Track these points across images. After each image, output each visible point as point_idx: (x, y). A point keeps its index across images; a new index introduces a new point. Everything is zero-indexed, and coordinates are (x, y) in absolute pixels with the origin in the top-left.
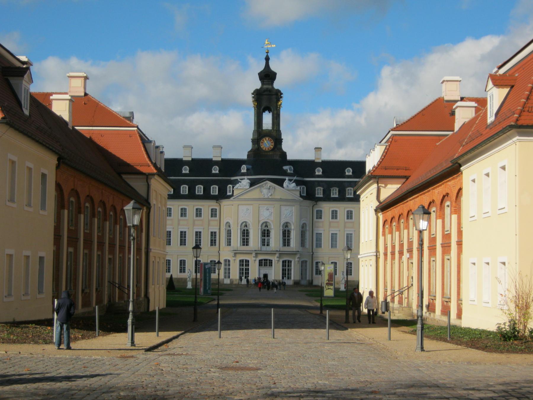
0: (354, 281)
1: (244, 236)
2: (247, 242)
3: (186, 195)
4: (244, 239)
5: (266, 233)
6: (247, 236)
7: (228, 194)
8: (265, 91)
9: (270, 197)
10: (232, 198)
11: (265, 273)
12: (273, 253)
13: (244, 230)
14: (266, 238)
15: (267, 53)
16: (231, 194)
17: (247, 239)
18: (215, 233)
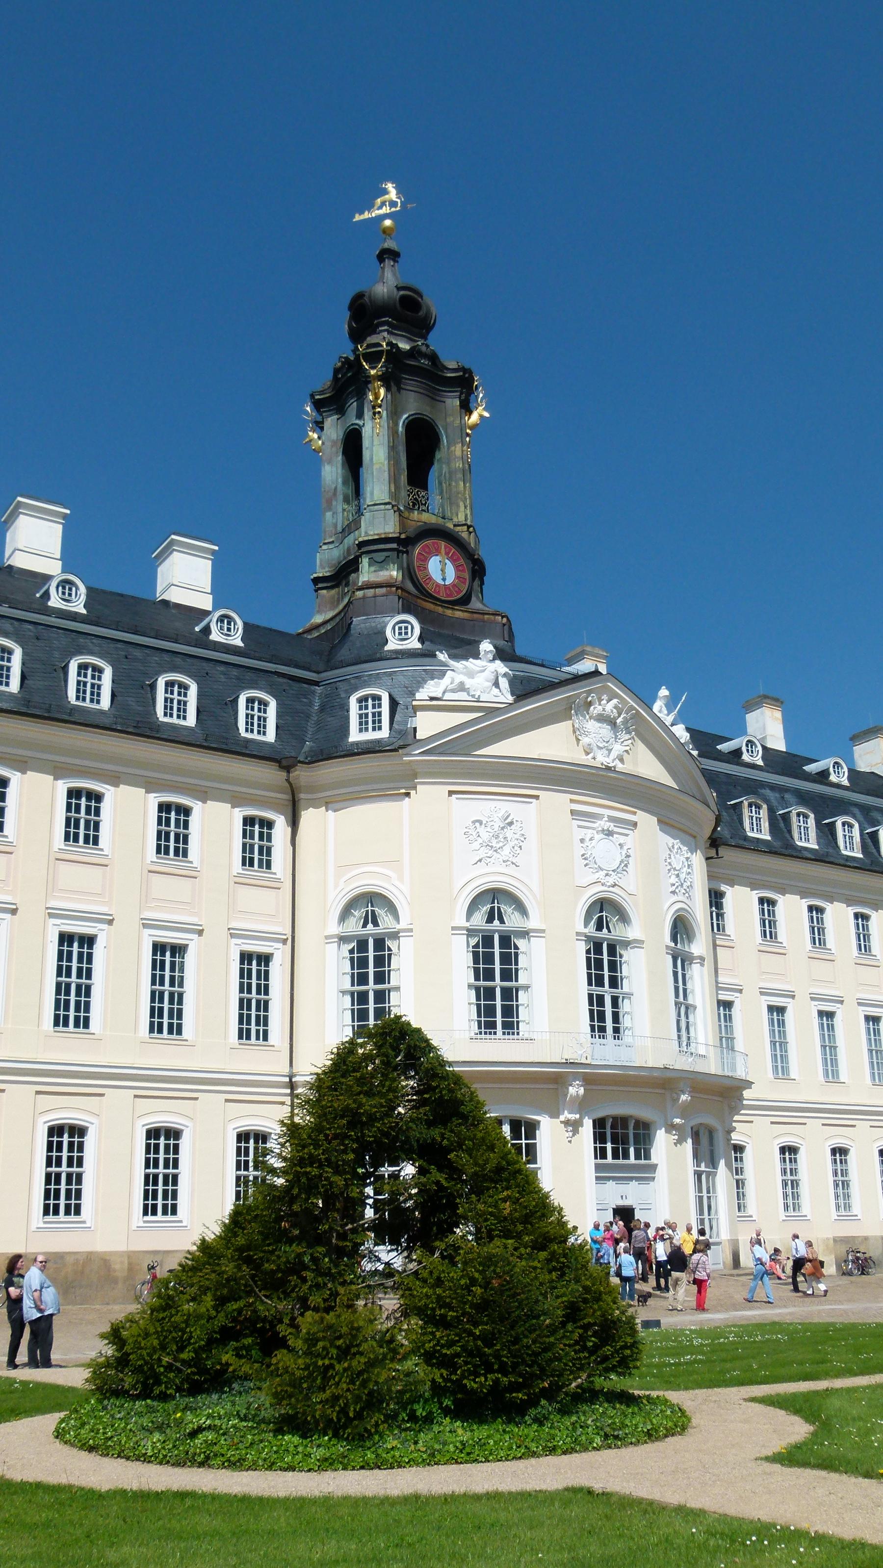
0: (866, 1238)
1: (489, 975)
2: (508, 1011)
3: (102, 712)
4: (490, 993)
5: (604, 963)
6: (507, 975)
7: (355, 736)
8: (414, 353)
9: (620, 767)
10: (415, 756)
11: (621, 1203)
12: (662, 1084)
13: (488, 941)
14: (607, 992)
15: (385, 231)
16: (384, 733)
17: (509, 994)
18: (265, 959)
